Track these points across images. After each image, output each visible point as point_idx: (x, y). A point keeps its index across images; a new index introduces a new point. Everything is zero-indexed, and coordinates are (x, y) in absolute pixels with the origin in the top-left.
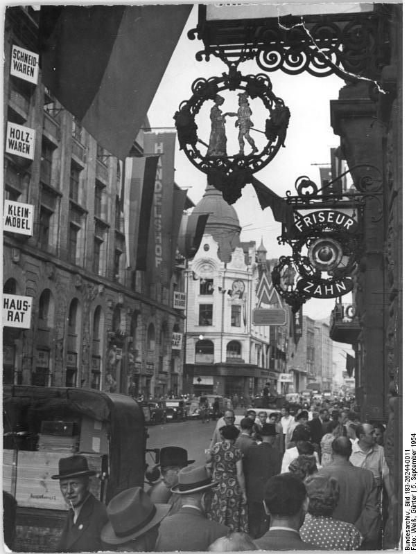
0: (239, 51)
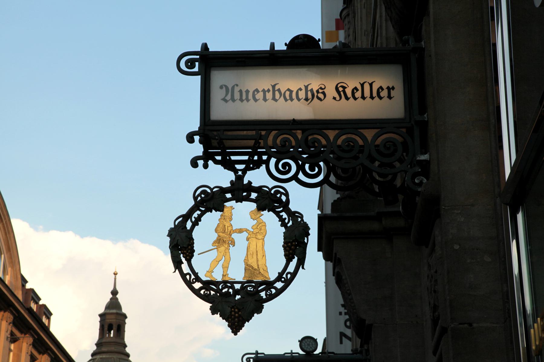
0: (246, 158)
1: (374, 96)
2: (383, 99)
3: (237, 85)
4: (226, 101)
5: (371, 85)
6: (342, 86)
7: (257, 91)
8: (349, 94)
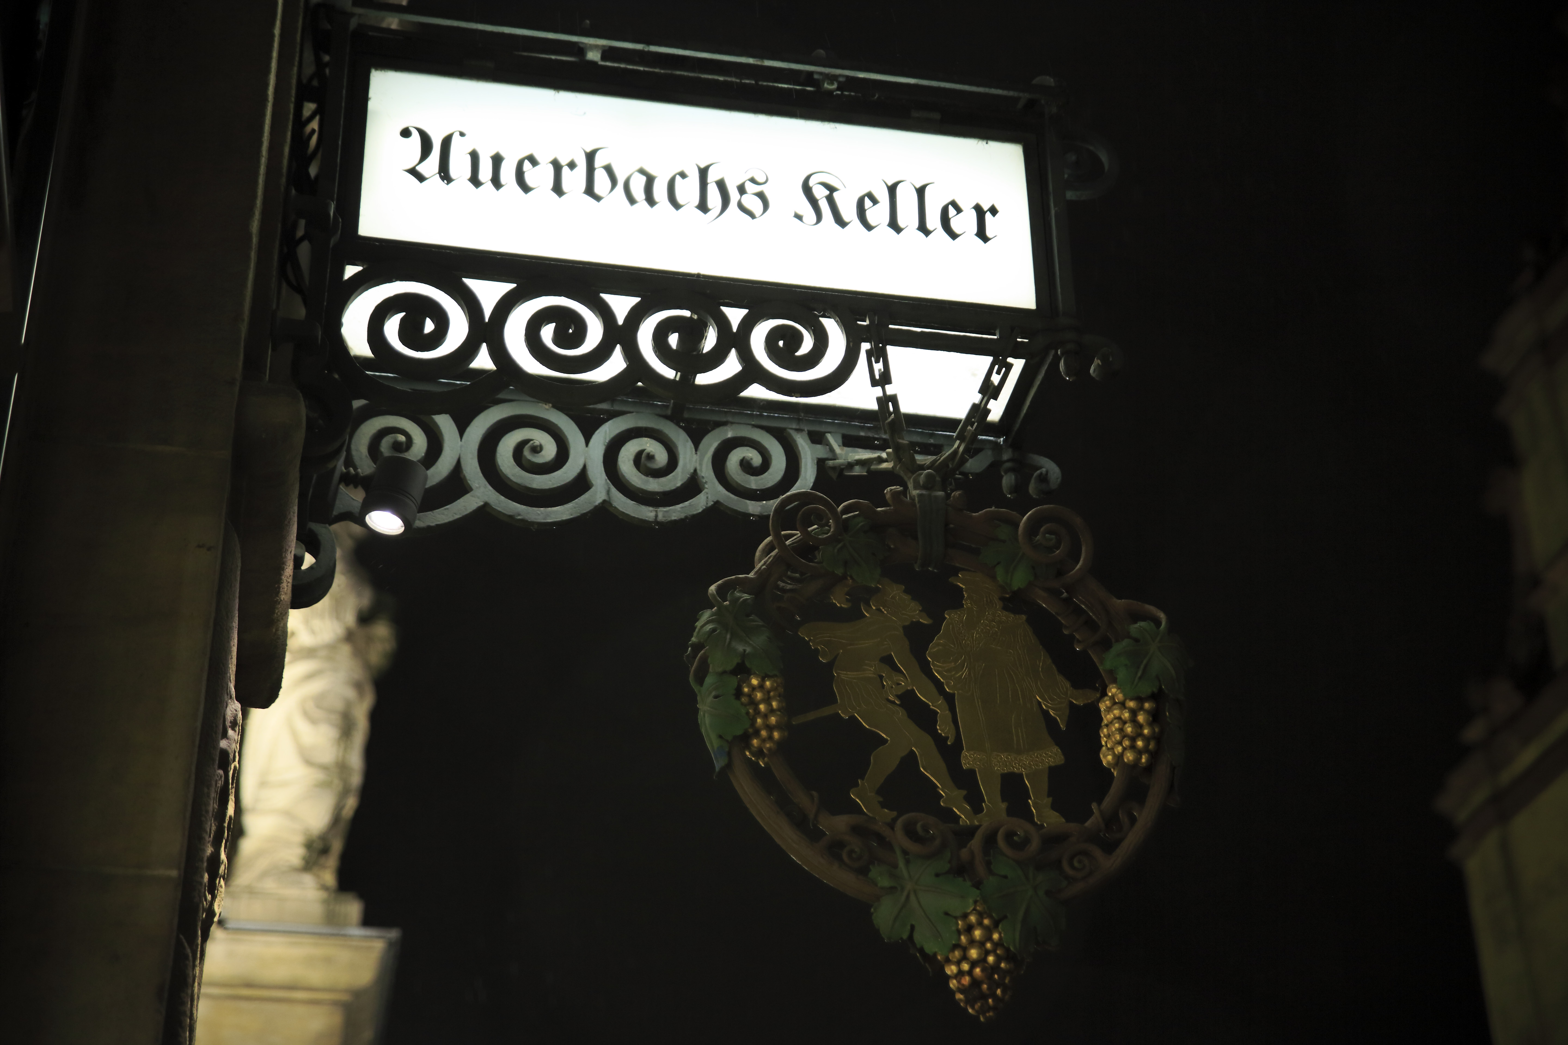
1: (930, 226)
3: (462, 134)
8: (849, 212)
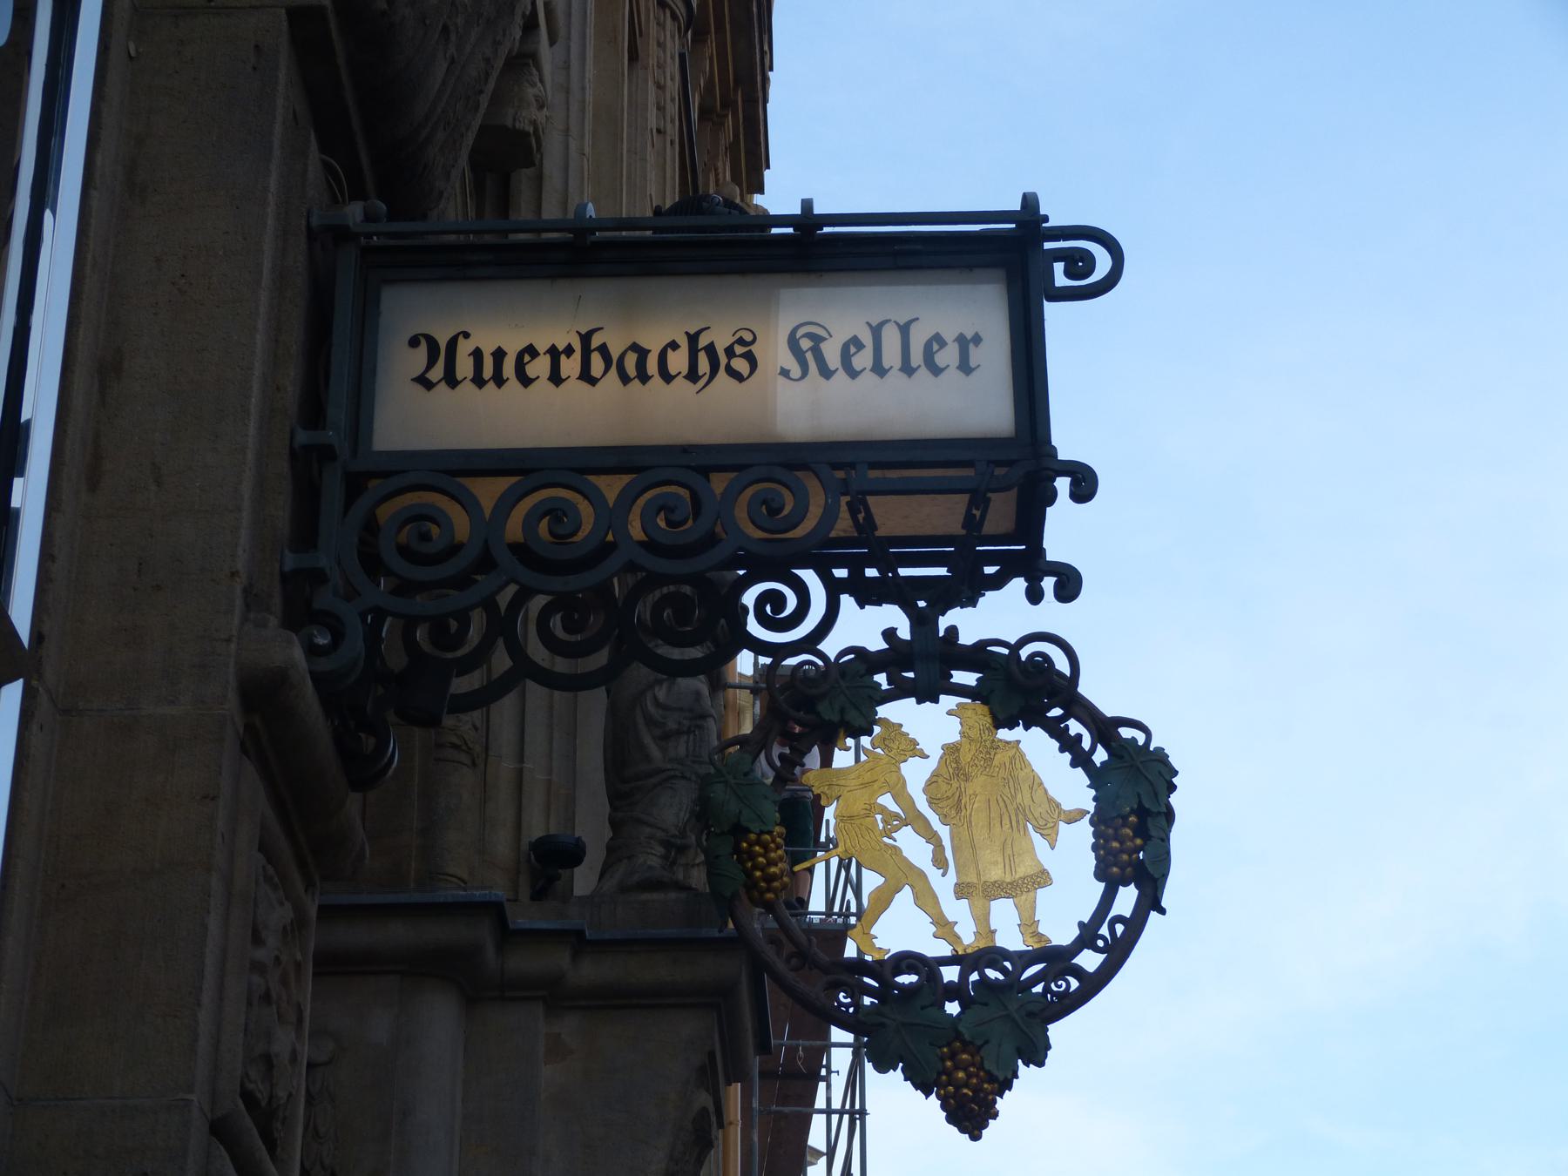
1: (914, 364)
2: (943, 376)
3: (466, 335)
4: (429, 385)
5: (905, 330)
6: (810, 336)
7: (531, 351)
